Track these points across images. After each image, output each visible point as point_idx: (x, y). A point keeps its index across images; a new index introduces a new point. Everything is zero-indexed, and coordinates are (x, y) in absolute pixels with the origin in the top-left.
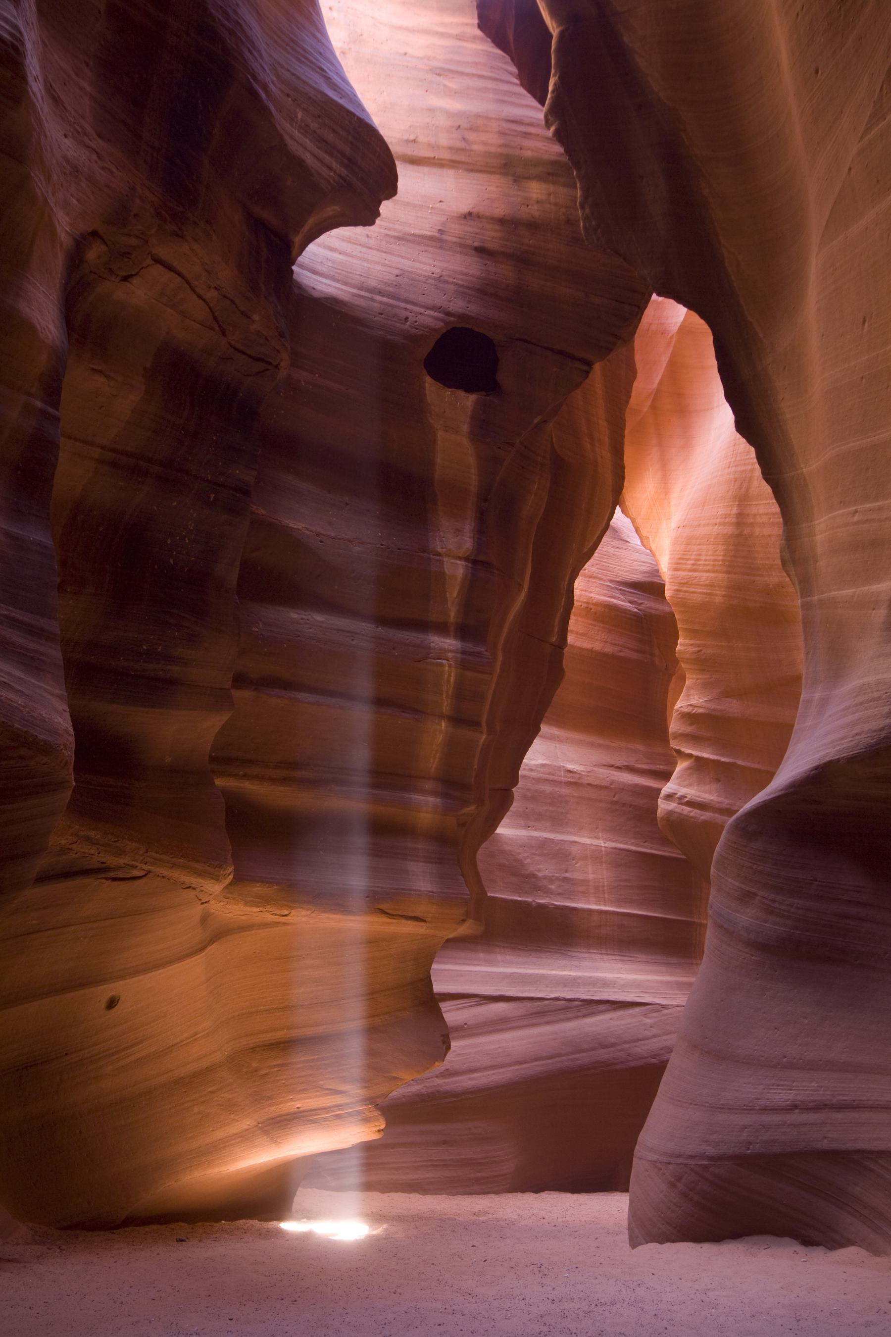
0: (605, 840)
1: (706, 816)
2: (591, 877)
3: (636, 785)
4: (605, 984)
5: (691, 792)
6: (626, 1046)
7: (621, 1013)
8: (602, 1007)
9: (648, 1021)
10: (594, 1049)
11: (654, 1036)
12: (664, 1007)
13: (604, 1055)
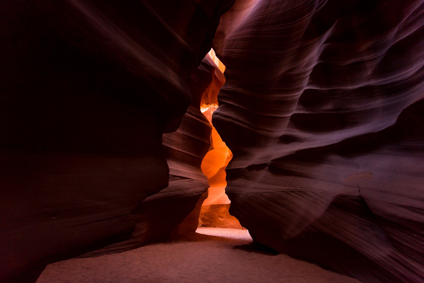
0: (181, 131)
1: (230, 120)
2: (176, 140)
3: (191, 118)
4: (178, 171)
5: (225, 113)
6: (184, 190)
7: (183, 180)
8: (178, 178)
9: (190, 183)
10: (176, 191)
11: (192, 188)
12: (194, 180)
13: (178, 192)
